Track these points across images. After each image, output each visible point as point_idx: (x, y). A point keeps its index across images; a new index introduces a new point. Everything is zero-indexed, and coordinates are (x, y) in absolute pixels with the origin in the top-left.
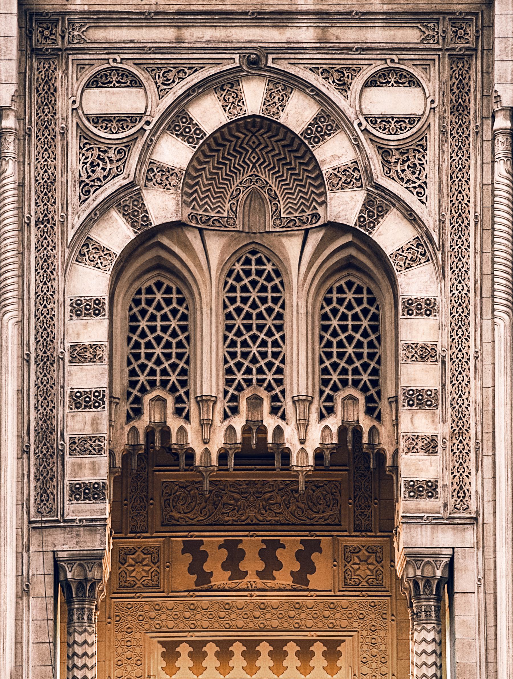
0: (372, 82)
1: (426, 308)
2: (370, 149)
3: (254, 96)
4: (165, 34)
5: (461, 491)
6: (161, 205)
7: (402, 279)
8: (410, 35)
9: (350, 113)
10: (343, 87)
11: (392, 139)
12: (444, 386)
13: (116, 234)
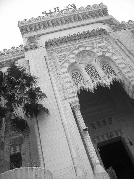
3: (82, 49)
4: (68, 47)
6: (72, 61)
13: (67, 65)
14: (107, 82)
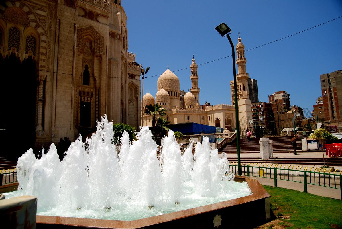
0: (38, 9)
1: (45, 42)
2: (37, 18)
5: (48, 68)
7: (41, 37)
8: (44, 5)
9: (35, 12)
10: (34, 8)
11: (41, 18)
12: (47, 53)
14: (23, 56)
